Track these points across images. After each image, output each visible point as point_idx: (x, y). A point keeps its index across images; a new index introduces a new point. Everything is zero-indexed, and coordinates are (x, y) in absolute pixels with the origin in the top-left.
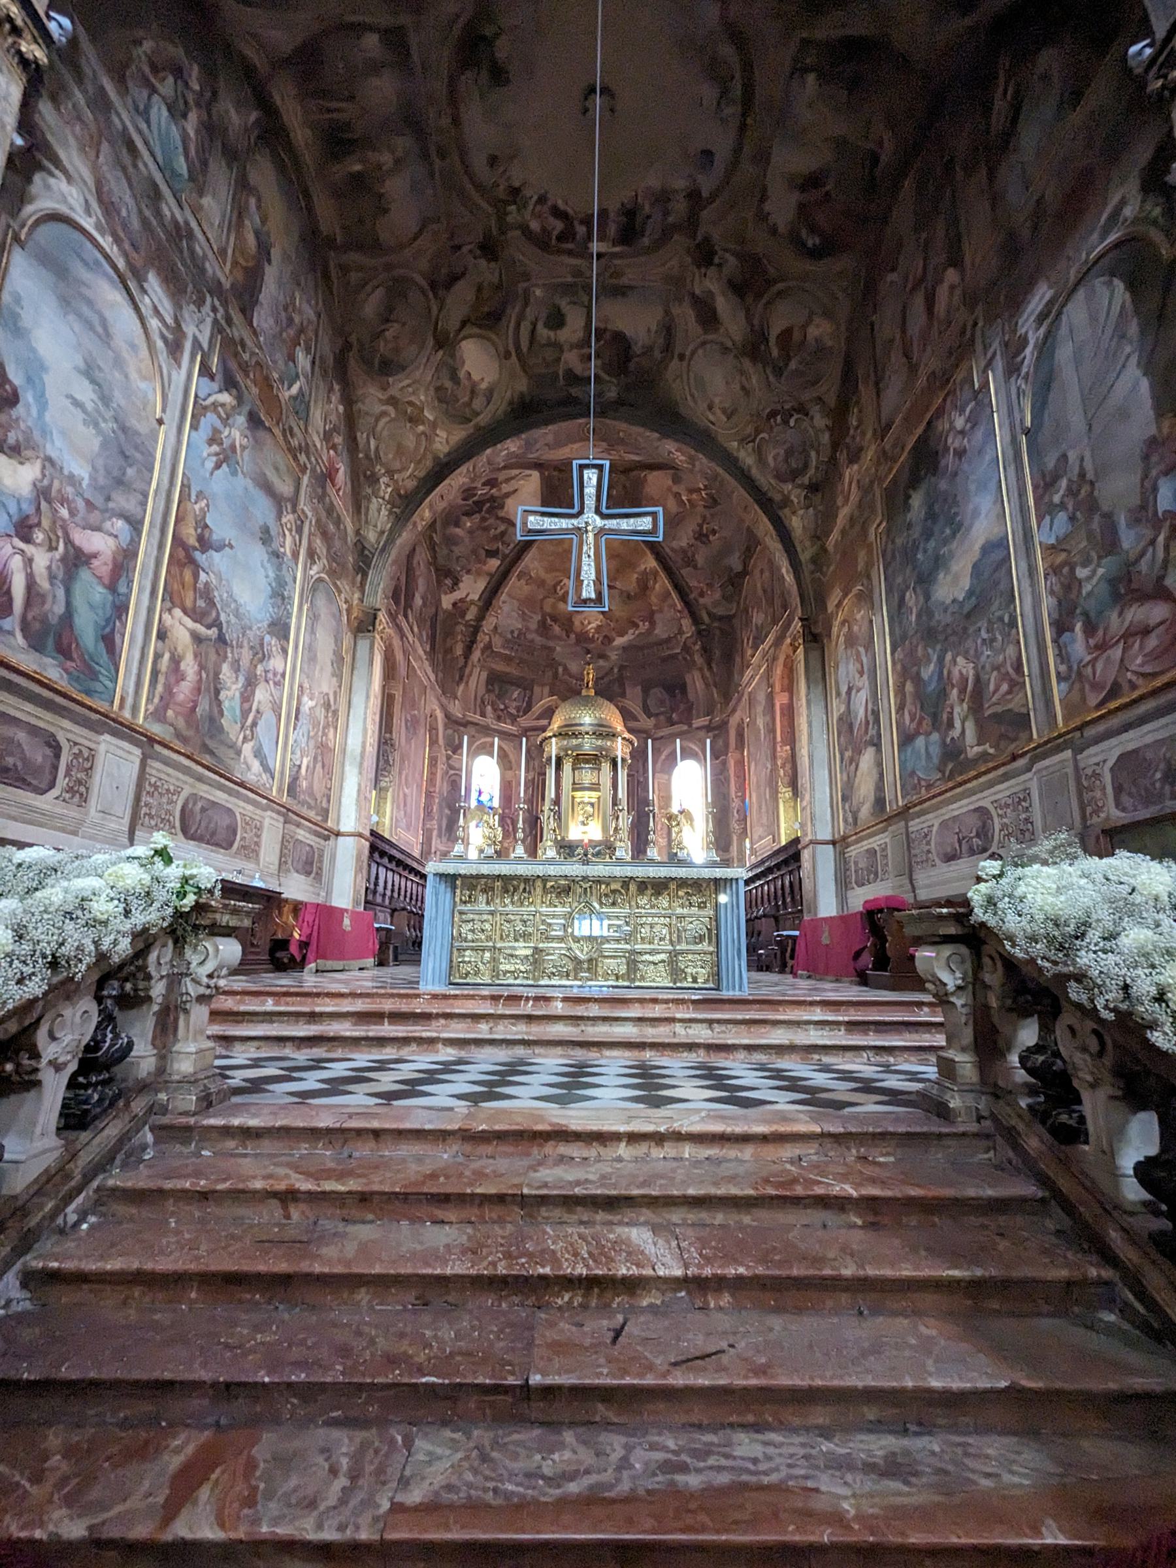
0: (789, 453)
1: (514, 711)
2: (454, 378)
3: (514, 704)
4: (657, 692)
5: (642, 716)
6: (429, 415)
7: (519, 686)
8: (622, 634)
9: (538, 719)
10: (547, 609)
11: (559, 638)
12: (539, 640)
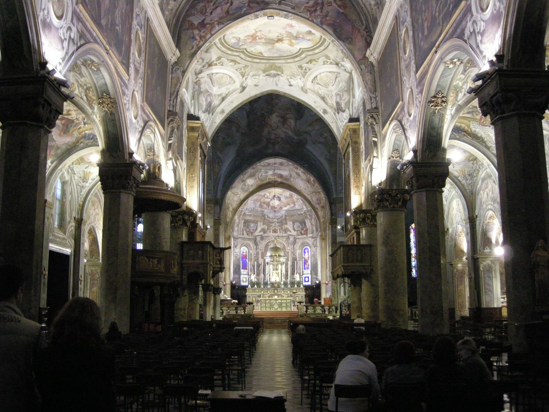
0: (317, 199)
1: (252, 231)
2: (245, 185)
3: (252, 228)
4: (297, 224)
5: (293, 231)
6: (240, 193)
7: (253, 223)
8: (285, 206)
9: (260, 232)
10: (262, 200)
11: (266, 208)
12: (259, 209)
